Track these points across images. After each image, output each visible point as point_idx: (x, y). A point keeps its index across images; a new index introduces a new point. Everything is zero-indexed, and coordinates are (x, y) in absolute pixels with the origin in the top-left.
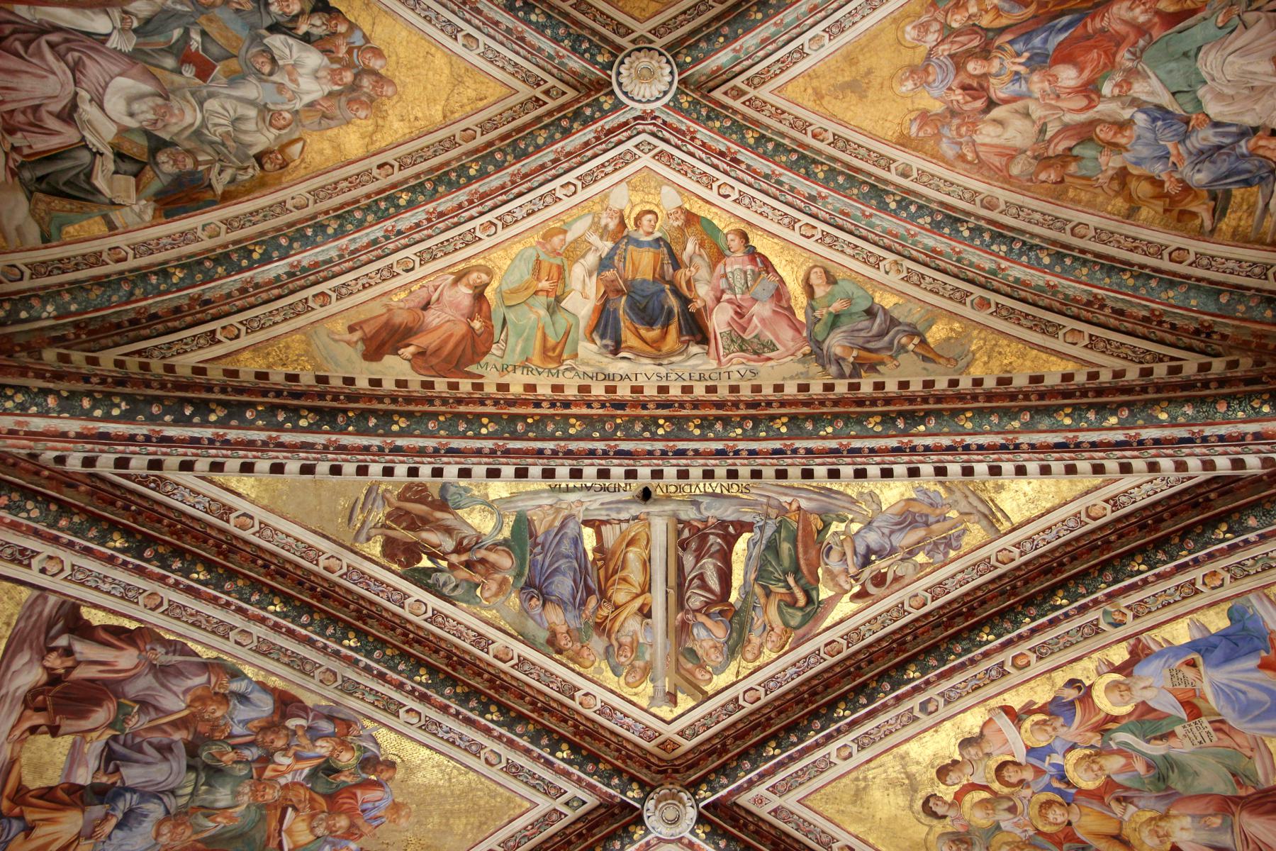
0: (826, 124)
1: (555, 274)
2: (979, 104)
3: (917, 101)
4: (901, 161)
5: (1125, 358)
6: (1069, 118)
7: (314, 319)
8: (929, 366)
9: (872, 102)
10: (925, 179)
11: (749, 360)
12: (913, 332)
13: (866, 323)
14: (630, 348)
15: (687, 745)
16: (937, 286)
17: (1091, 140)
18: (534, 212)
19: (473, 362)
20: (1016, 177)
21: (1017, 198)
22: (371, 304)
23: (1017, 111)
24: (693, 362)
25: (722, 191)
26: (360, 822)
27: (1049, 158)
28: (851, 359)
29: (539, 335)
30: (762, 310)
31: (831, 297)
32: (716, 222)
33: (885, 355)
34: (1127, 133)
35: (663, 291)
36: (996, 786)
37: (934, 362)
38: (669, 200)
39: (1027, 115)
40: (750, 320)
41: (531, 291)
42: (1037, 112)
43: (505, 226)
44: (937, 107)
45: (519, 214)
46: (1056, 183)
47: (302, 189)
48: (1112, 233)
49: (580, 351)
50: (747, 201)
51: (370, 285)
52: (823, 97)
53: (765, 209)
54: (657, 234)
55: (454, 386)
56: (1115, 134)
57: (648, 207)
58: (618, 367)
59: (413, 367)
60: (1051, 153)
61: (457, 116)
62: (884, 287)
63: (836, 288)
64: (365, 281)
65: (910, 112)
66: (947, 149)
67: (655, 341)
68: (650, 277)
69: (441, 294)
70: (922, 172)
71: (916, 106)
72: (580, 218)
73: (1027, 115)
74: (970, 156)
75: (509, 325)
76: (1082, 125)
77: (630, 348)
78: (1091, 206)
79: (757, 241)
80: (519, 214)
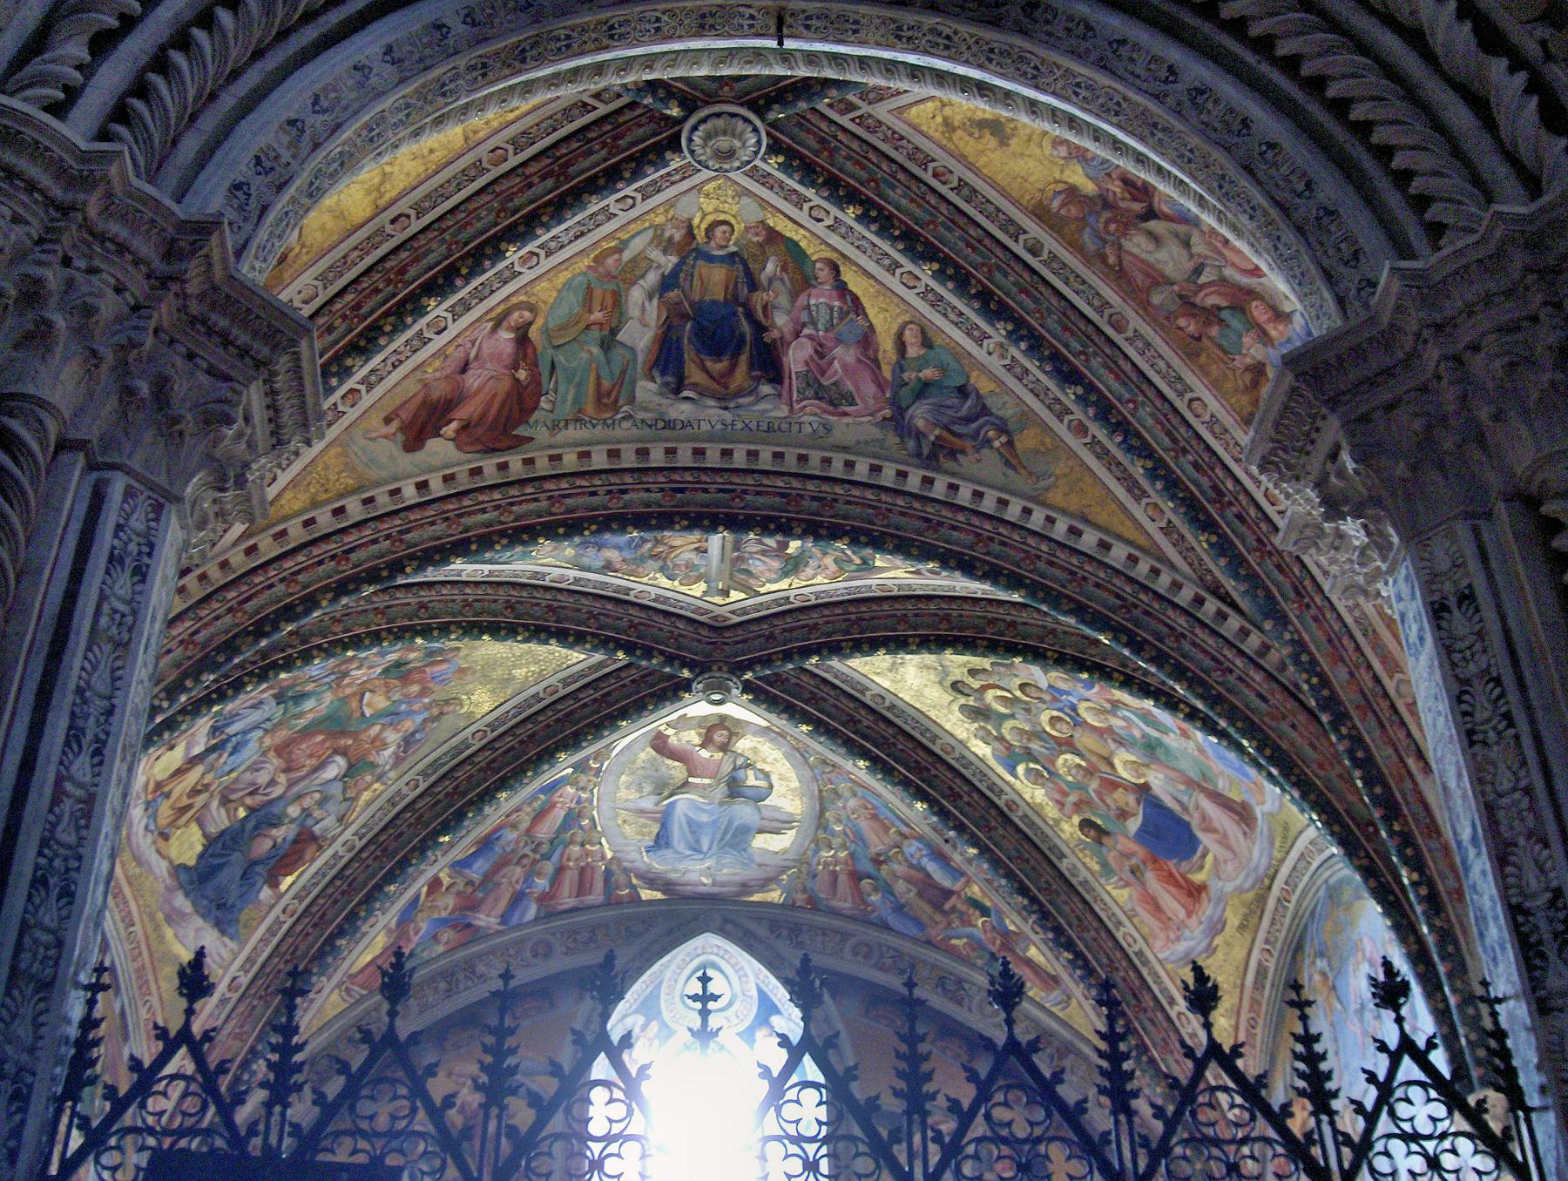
0: (952, 164)
1: (609, 301)
2: (1137, 207)
3: (1067, 172)
4: (1033, 234)
5: (1190, 565)
6: (1228, 272)
7: (346, 424)
8: (1010, 472)
9: (1013, 154)
10: (1055, 265)
11: (825, 411)
12: (1003, 429)
13: (956, 401)
14: (694, 387)
15: (736, 619)
16: (1039, 388)
17: (1243, 310)
18: (583, 234)
19: (519, 423)
20: (1154, 307)
21: (1147, 331)
22: (406, 382)
23: (1177, 235)
24: (762, 406)
25: (814, 213)
26: (431, 685)
27: (1194, 305)
28: (932, 438)
29: (592, 378)
30: (844, 356)
31: (923, 362)
32: (803, 244)
33: (968, 444)
34: (1281, 328)
35: (735, 314)
36: (1018, 693)
37: (1015, 469)
38: (752, 212)
39: (1187, 244)
40: (831, 363)
41: (582, 326)
42: (1199, 247)
43: (549, 254)
44: (1089, 187)
45: (564, 239)
46: (1192, 337)
47: (308, 277)
48: (1226, 431)
49: (639, 393)
50: (843, 230)
51: (401, 362)
52: (954, 130)
53: (864, 243)
54: (733, 249)
55: (503, 467)
56: (1269, 320)
57: (722, 217)
58: (681, 410)
59: (459, 448)
60: (1198, 300)
61: (481, 135)
62: (983, 369)
63: (932, 353)
64: (393, 359)
65: (1057, 182)
66: (1087, 239)
67: (723, 376)
68: (721, 298)
69: (480, 349)
70: (1053, 257)
71: (1064, 178)
72: (639, 233)
73: (1187, 244)
74: (1112, 260)
75: (559, 371)
76: (1241, 289)
77: (694, 387)
78: (1216, 385)
79: (849, 276)
80: (564, 239)
